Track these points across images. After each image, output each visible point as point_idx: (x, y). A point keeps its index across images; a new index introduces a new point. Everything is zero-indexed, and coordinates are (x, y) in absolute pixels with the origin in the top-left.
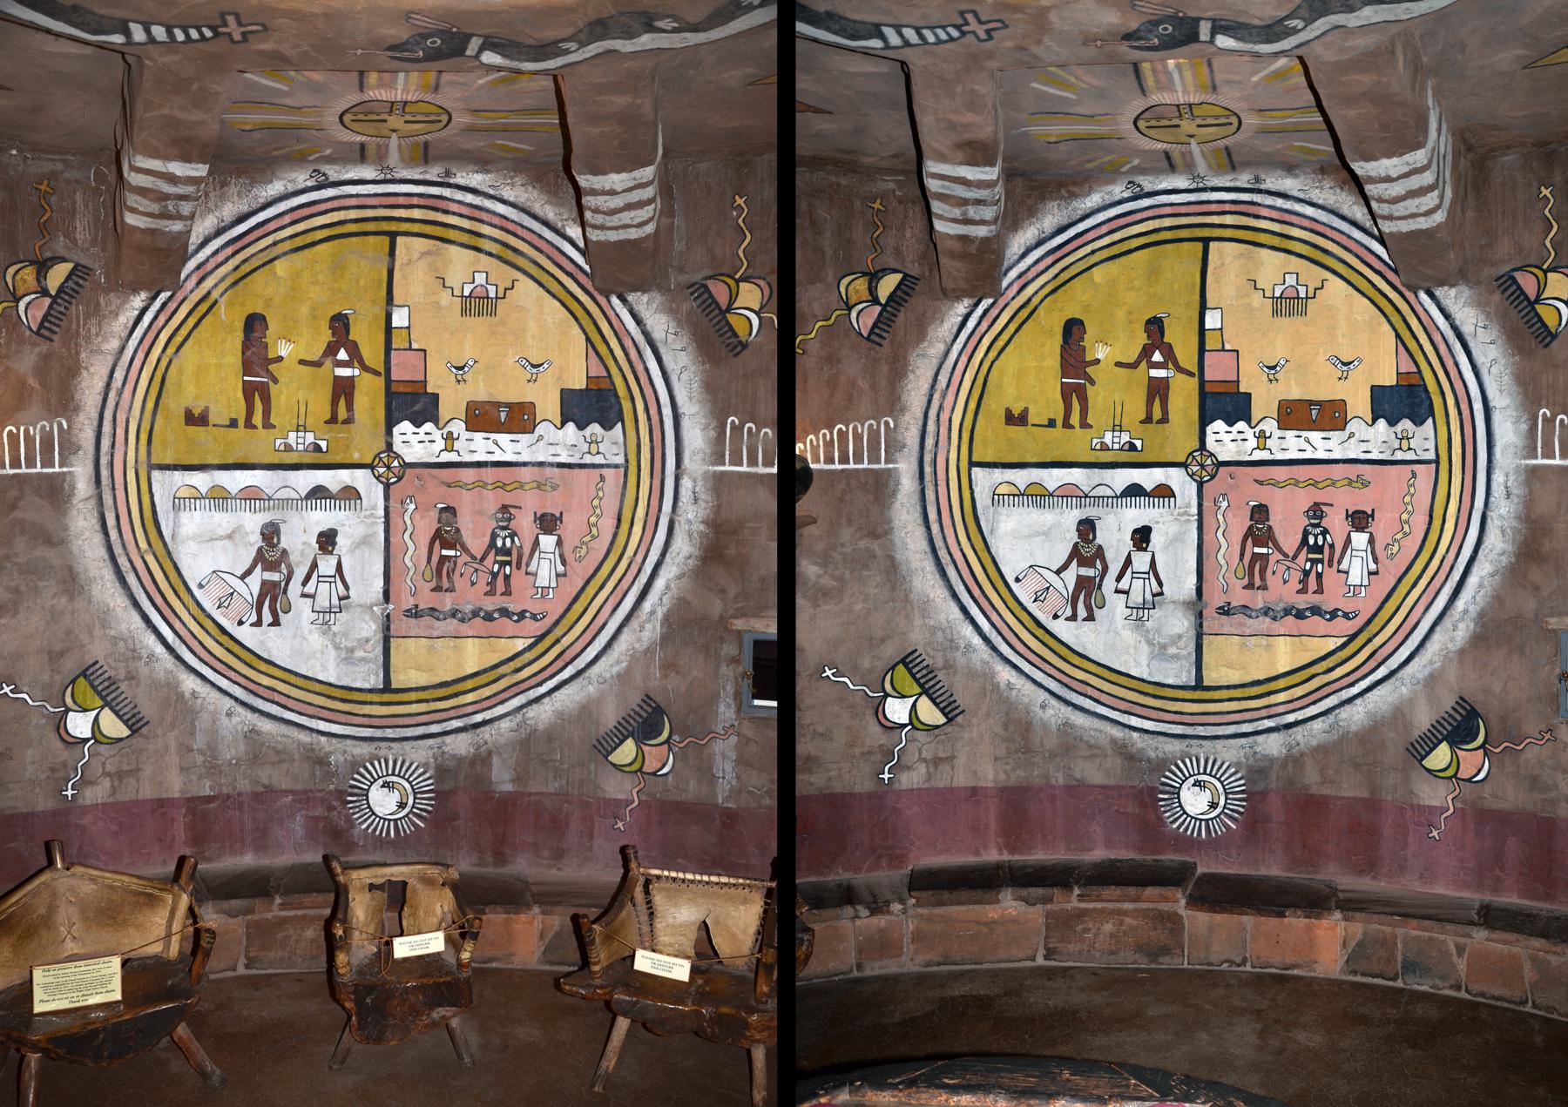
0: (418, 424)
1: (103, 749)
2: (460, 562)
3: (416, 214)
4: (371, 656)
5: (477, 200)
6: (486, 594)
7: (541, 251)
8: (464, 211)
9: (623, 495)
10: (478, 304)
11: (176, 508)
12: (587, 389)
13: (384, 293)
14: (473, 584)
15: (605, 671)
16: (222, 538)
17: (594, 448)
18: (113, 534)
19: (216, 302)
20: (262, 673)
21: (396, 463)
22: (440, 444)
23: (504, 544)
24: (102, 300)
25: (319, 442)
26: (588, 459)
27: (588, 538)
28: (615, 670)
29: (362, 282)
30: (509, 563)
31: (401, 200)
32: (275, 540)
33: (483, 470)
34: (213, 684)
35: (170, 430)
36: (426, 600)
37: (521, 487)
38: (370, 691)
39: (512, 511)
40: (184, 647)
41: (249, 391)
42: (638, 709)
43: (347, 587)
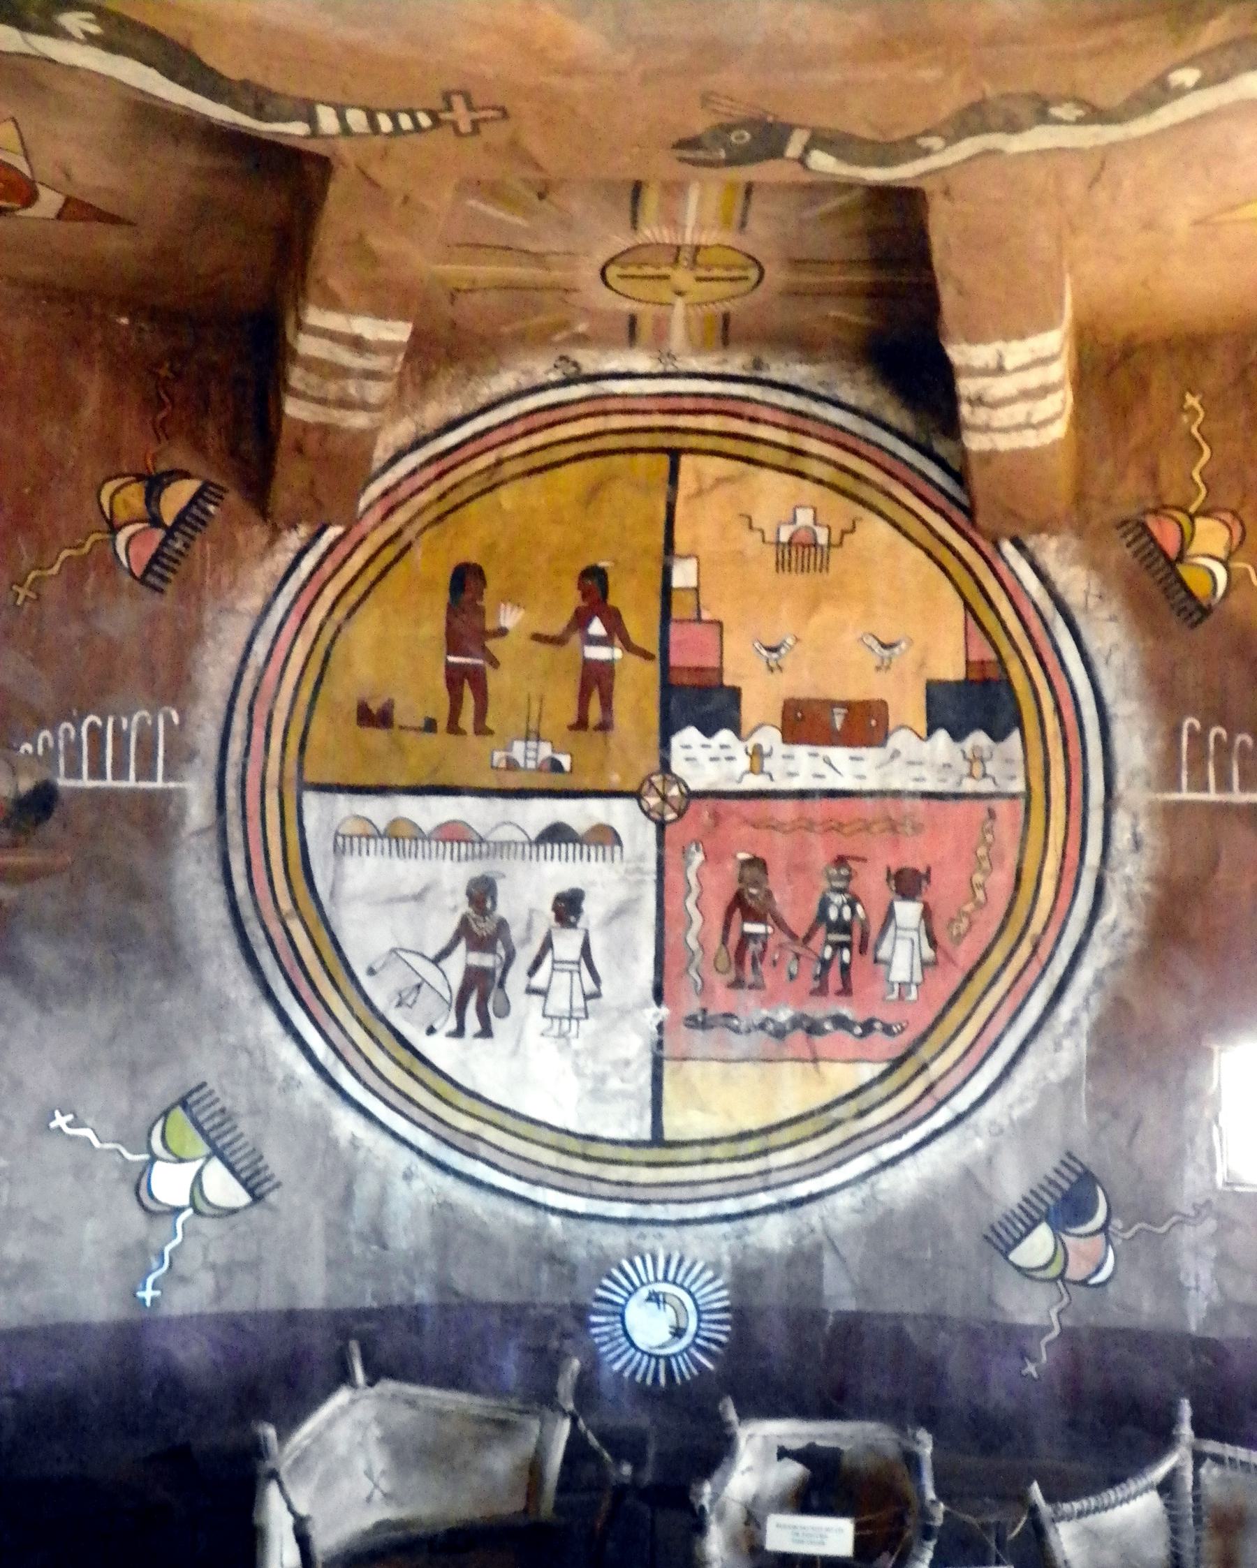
0: (708, 730)
1: (206, 1226)
2: (772, 943)
3: (710, 422)
4: (630, 1087)
9: (1024, 840)
11: (339, 851)
12: (967, 682)
13: (661, 540)
14: (792, 977)
16: (403, 899)
17: (977, 770)
18: (241, 886)
20: (460, 1110)
22: (743, 762)
23: (840, 915)
24: (240, 537)
26: (969, 786)
28: (1017, 1113)
30: (848, 945)
31: (688, 404)
32: (489, 905)
33: (808, 802)
36: (723, 999)
38: (631, 1144)
39: (852, 864)
40: (341, 1068)
41: (455, 678)
42: (1053, 1176)
43: (596, 979)
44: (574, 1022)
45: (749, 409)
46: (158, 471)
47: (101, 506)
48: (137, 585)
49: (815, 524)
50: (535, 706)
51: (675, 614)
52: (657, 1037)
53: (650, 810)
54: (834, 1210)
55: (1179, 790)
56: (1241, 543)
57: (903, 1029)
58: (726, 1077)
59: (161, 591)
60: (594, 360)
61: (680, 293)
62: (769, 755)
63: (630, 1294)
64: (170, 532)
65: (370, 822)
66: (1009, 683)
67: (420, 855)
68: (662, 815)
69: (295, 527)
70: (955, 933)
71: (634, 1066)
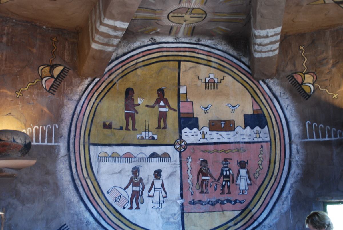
0: (191, 129)
2: (210, 181)
3: (187, 54)
4: (176, 221)
6: (221, 194)
7: (233, 66)
8: (204, 53)
9: (270, 153)
10: (211, 85)
11: (99, 161)
12: (253, 114)
13: (177, 81)
14: (215, 190)
16: (116, 173)
19: (115, 83)
21: (183, 144)
22: (200, 136)
25: (154, 136)
26: (256, 140)
27: (258, 170)
28: (274, 221)
29: (169, 77)
30: (229, 181)
31: (182, 49)
35: (97, 131)
36: (198, 197)
37: (231, 151)
39: (229, 160)
40: (101, 218)
41: (127, 116)
43: (166, 193)
44: (161, 204)
45: (197, 51)
46: (53, 64)
47: (39, 72)
48: (47, 93)
50: (147, 123)
51: (181, 100)
52: (182, 207)
53: (177, 149)
55: (307, 139)
57: (244, 202)
59: (54, 94)
60: (159, 39)
61: (185, 21)
64: (56, 79)
65: (107, 153)
67: (120, 162)
68: (180, 150)
69: (87, 78)
70: (255, 176)
71: (177, 215)
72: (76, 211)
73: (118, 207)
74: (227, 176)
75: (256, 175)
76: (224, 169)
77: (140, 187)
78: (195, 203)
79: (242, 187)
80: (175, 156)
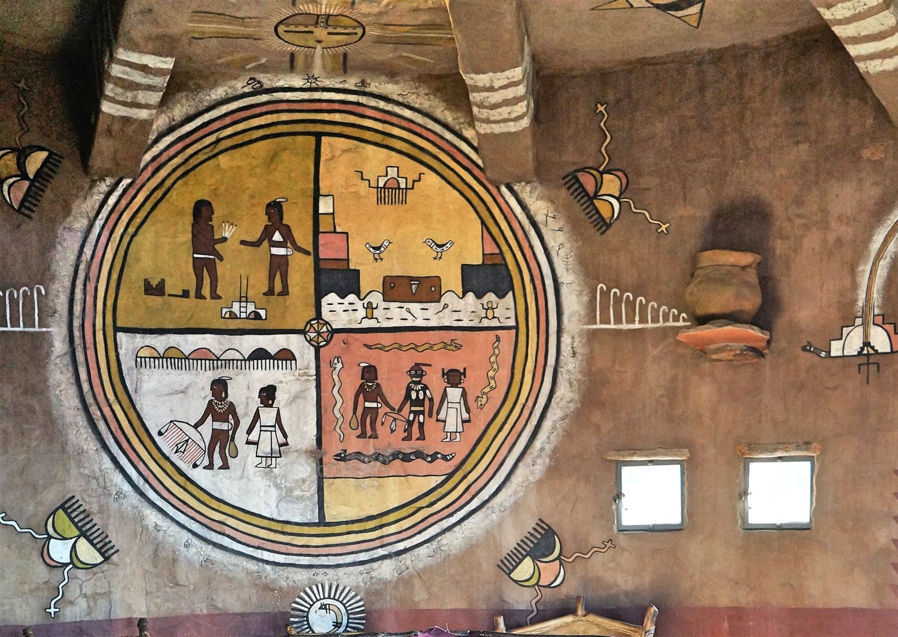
1: (80, 573)
2: (381, 412)
4: (307, 494)
5: (389, 107)
6: (403, 439)
12: (483, 264)
13: (312, 186)
14: (392, 431)
15: (506, 501)
16: (177, 393)
21: (324, 329)
22: (362, 313)
25: (258, 311)
26: (486, 323)
30: (423, 413)
34: (173, 520)
36: (354, 445)
37: (431, 348)
39: (424, 368)
40: (147, 486)
49: (398, 177)
50: (244, 282)
53: (311, 340)
54: (418, 555)
55: (595, 323)
56: (626, 188)
57: (453, 457)
58: (358, 487)
62: (376, 308)
63: (311, 606)
66: (506, 265)
68: (318, 344)
70: (479, 403)
71: (308, 482)
72: (94, 471)
73: (183, 463)
74: (419, 402)
75: (481, 400)
76: (412, 385)
77: (229, 422)
78: (348, 458)
79: (451, 426)
80: (306, 356)
